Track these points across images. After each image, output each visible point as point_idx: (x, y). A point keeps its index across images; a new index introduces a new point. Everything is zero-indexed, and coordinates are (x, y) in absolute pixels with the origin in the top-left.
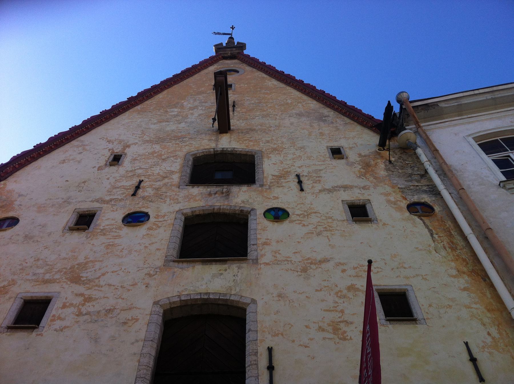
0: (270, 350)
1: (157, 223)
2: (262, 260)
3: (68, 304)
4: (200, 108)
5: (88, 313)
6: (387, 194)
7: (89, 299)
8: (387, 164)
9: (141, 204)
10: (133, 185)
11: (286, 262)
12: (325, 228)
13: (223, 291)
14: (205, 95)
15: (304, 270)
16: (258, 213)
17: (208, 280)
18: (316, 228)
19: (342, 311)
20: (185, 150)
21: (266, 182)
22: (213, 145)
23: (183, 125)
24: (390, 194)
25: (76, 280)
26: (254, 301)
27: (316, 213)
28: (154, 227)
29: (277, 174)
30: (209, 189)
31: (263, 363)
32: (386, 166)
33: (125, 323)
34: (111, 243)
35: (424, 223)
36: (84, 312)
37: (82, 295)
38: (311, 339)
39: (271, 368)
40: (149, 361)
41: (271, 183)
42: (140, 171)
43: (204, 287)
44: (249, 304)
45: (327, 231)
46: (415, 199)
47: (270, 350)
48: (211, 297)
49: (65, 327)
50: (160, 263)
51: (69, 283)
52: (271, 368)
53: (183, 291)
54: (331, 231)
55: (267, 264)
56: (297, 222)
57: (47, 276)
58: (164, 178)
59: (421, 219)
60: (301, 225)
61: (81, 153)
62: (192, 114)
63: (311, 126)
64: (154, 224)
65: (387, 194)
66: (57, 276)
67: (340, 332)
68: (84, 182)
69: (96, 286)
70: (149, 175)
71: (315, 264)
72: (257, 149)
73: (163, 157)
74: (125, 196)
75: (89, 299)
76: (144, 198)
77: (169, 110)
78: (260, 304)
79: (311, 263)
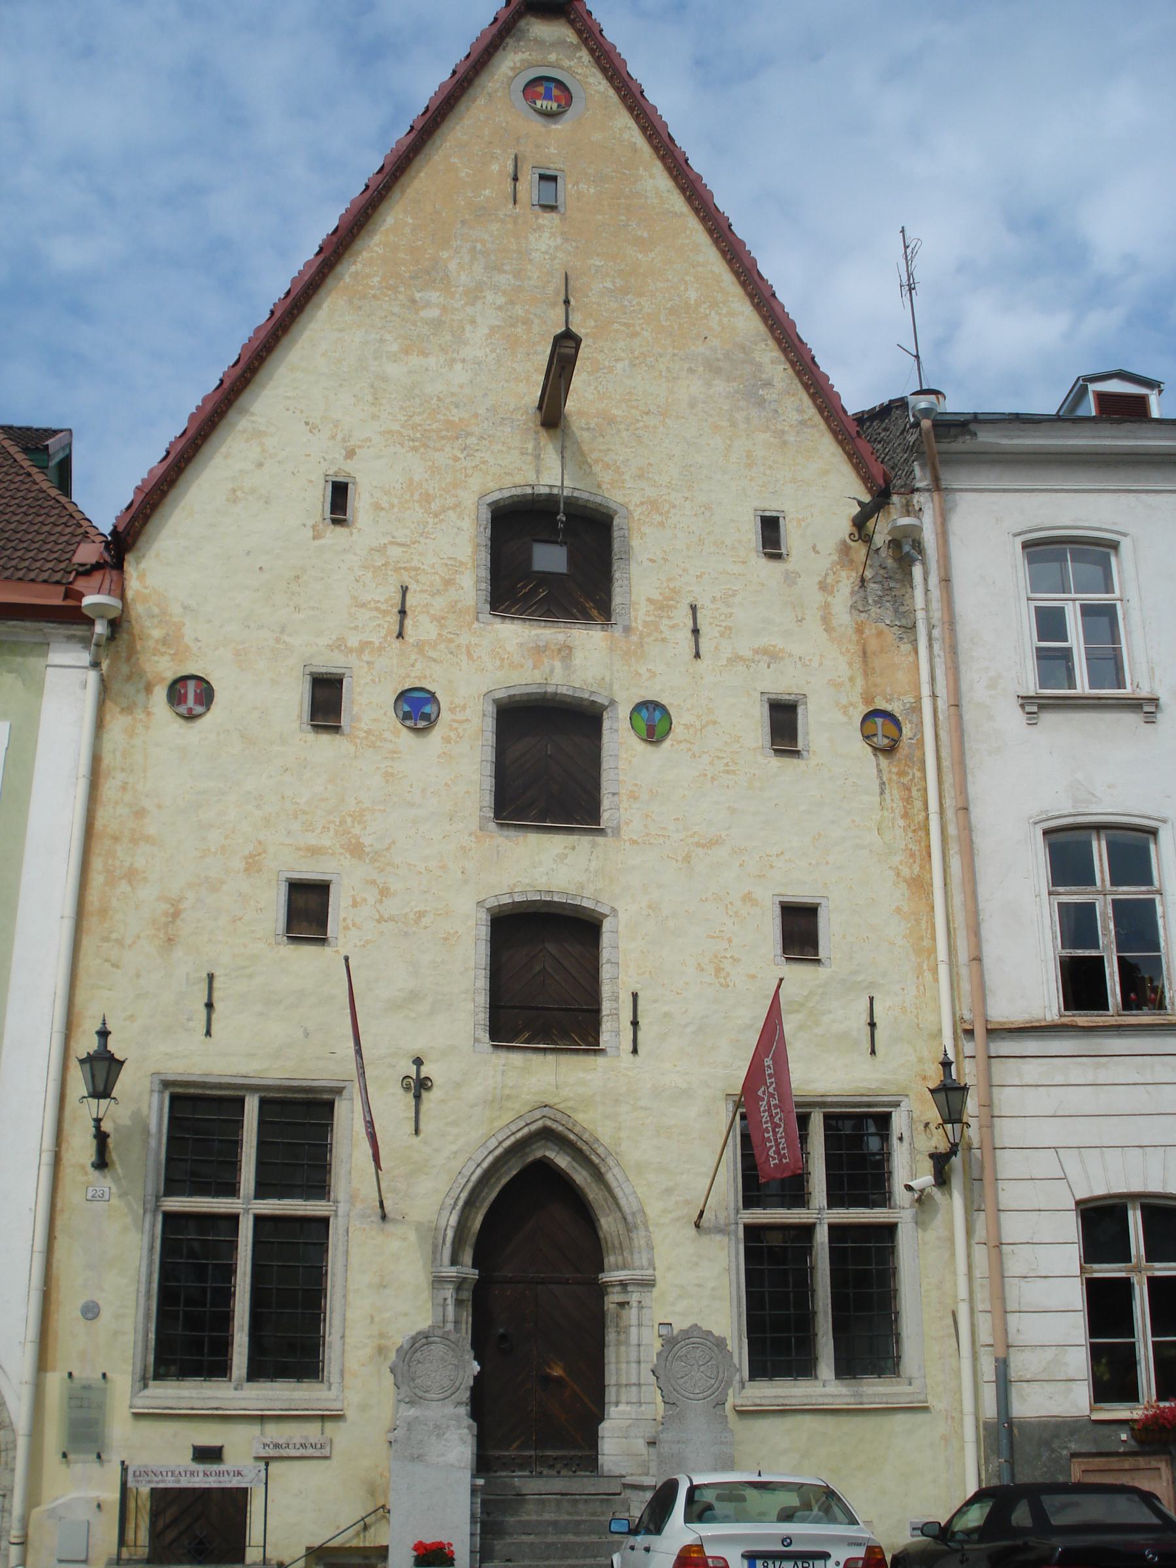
0: (635, 996)
1: (455, 725)
2: (626, 833)
3: (358, 900)
4: (490, 296)
5: (391, 919)
6: (836, 685)
7: (384, 892)
8: (856, 588)
9: (418, 665)
10: (390, 598)
11: (661, 840)
12: (727, 765)
13: (572, 890)
14: (495, 227)
15: (687, 859)
16: (620, 716)
17: (545, 865)
18: (712, 763)
19: (730, 941)
20: (476, 484)
21: (636, 618)
22: (531, 478)
23: (460, 375)
24: (841, 685)
25: (356, 850)
26: (614, 910)
27: (715, 723)
28: (452, 735)
29: (656, 596)
30: (534, 632)
31: (626, 1016)
32: (852, 593)
33: (446, 939)
34: (390, 770)
35: (878, 765)
36: (386, 917)
37: (373, 882)
38: (687, 984)
39: (635, 1023)
40: (483, 999)
41: (646, 624)
42: (395, 552)
43: (544, 880)
44: (607, 916)
45: (728, 772)
46: (881, 704)
47: (635, 996)
48: (556, 899)
49: (367, 942)
50: (474, 825)
51: (348, 856)
52: (635, 1023)
53: (515, 885)
54: (734, 772)
55: (634, 842)
56: (684, 746)
57: (312, 840)
58: (448, 583)
59: (875, 755)
60: (690, 753)
61: (260, 465)
62: (473, 322)
63: (734, 424)
64: (451, 728)
65: (836, 685)
66: (326, 841)
67: (723, 974)
68: (297, 577)
69: (389, 864)
70: (416, 569)
71: (703, 846)
72: (620, 499)
73: (434, 506)
74: (385, 638)
75: (384, 892)
76: (420, 647)
77: (418, 296)
78: (623, 917)
79: (698, 844)
